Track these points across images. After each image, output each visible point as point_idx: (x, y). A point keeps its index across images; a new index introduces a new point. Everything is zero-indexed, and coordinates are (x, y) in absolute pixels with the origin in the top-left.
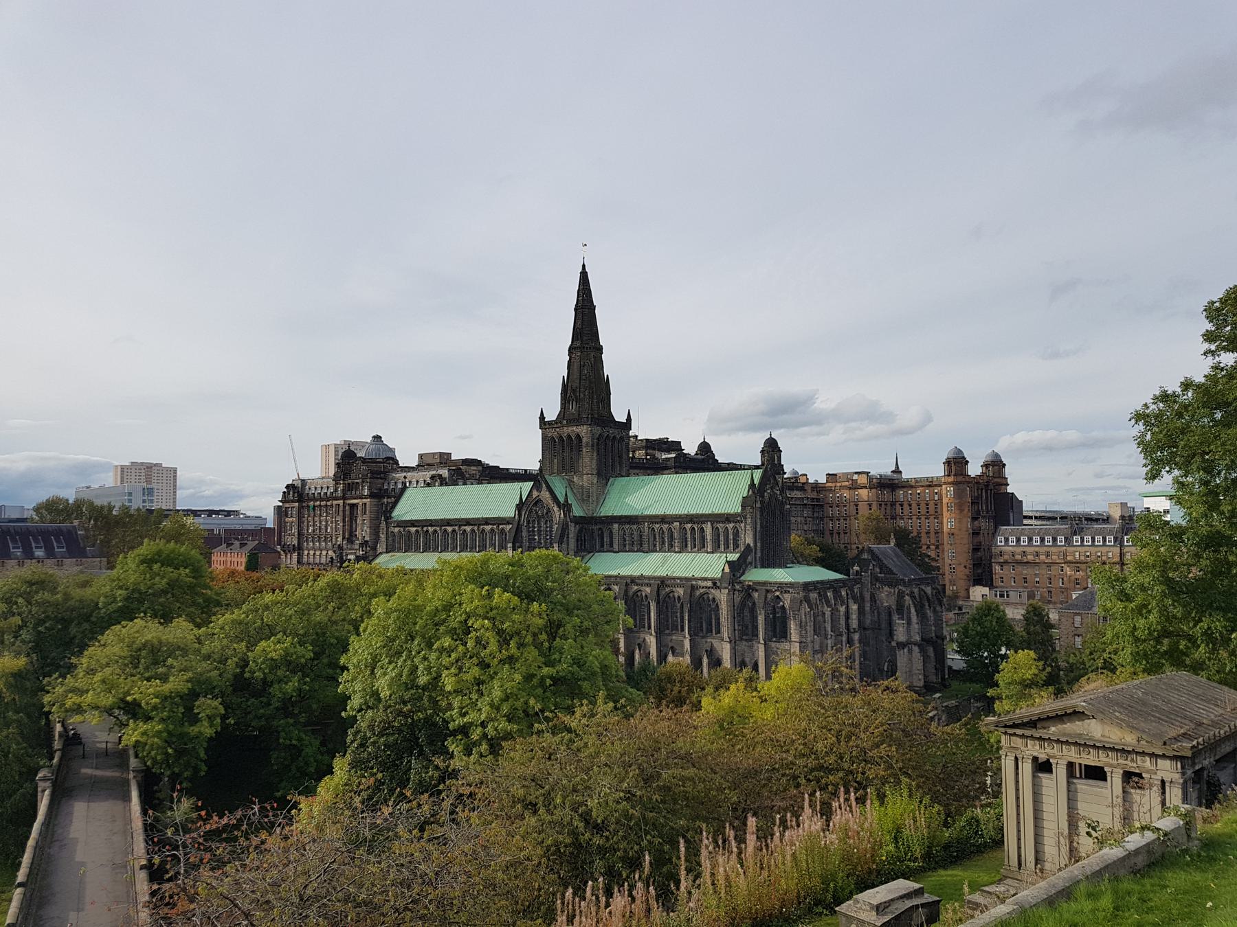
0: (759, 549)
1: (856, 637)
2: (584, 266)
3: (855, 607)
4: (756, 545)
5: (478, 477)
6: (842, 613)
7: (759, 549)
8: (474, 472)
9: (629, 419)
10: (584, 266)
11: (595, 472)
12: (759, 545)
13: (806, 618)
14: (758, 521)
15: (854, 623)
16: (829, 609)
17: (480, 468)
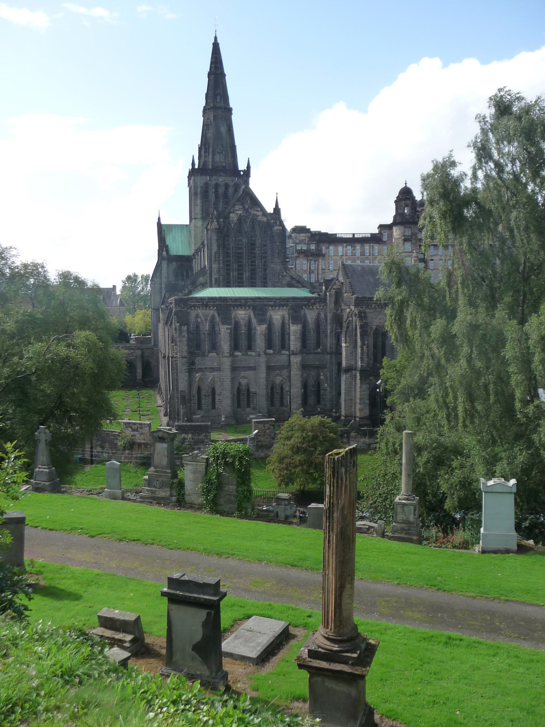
0: (215, 271)
1: (296, 360)
2: (216, 38)
3: (294, 329)
4: (211, 268)
5: (307, 241)
6: (258, 333)
7: (215, 271)
8: (303, 238)
9: (249, 167)
10: (216, 38)
11: (199, 216)
12: (215, 266)
13: (176, 333)
14: (214, 241)
15: (294, 343)
16: (226, 327)
17: (309, 235)
